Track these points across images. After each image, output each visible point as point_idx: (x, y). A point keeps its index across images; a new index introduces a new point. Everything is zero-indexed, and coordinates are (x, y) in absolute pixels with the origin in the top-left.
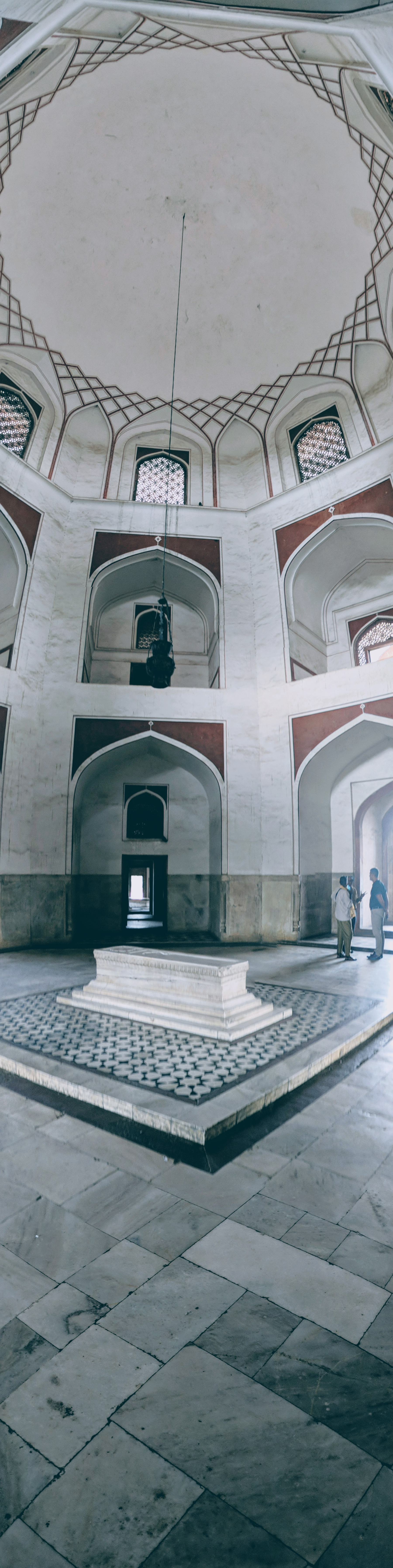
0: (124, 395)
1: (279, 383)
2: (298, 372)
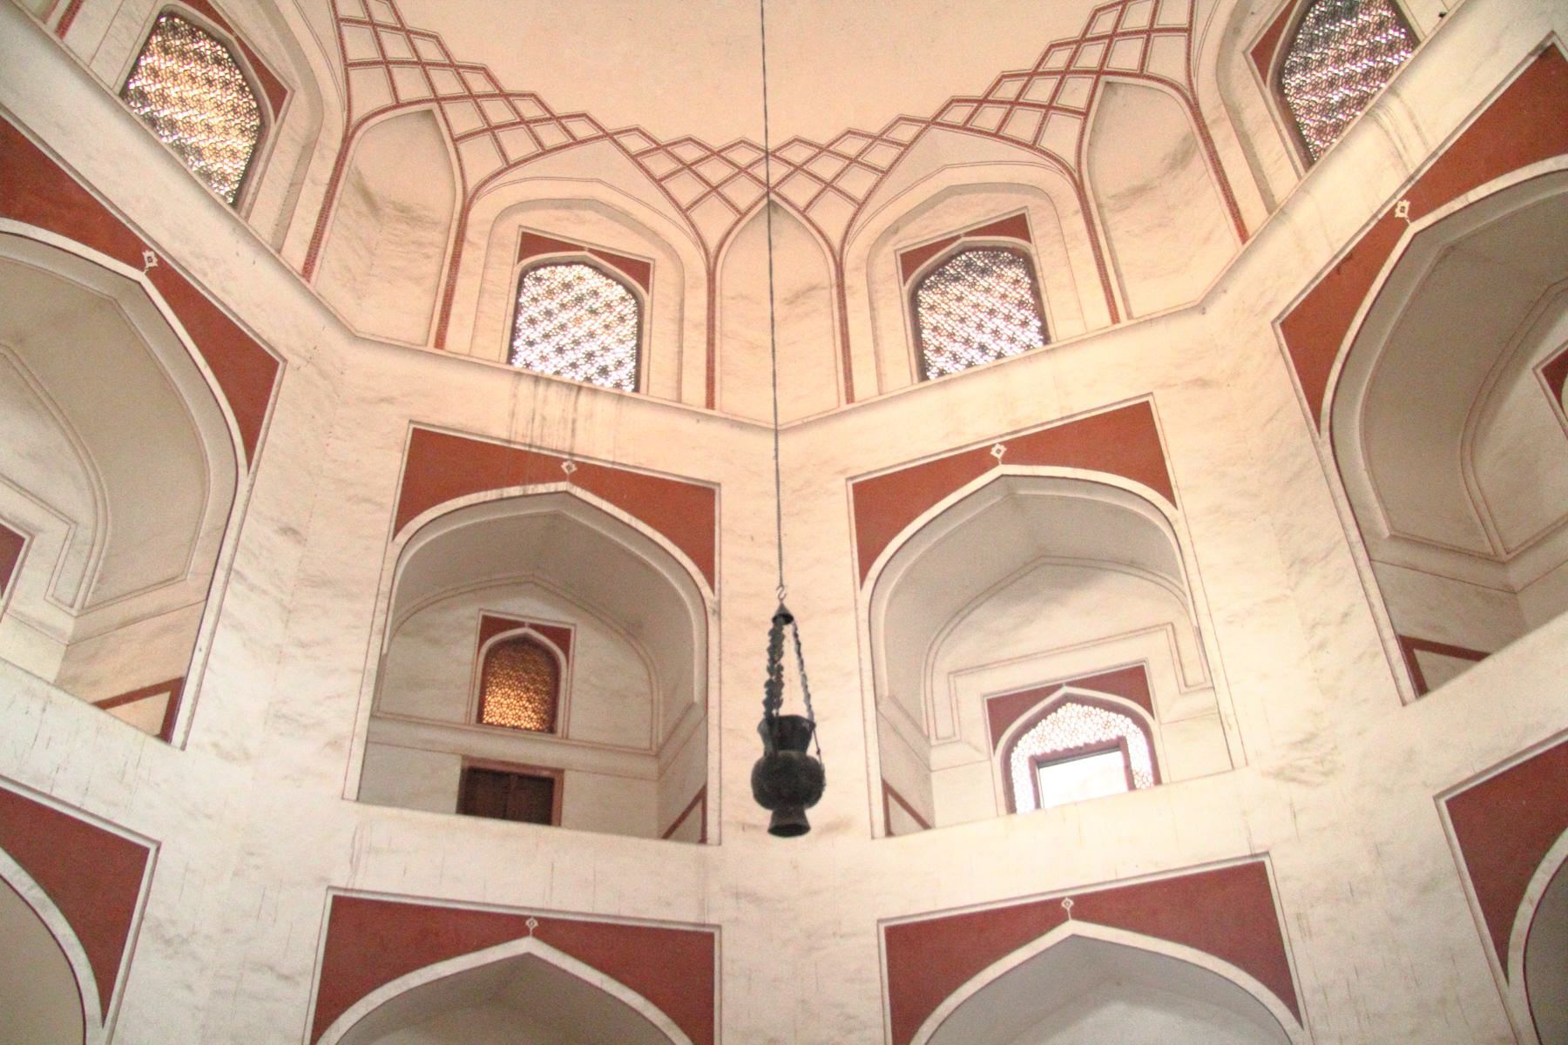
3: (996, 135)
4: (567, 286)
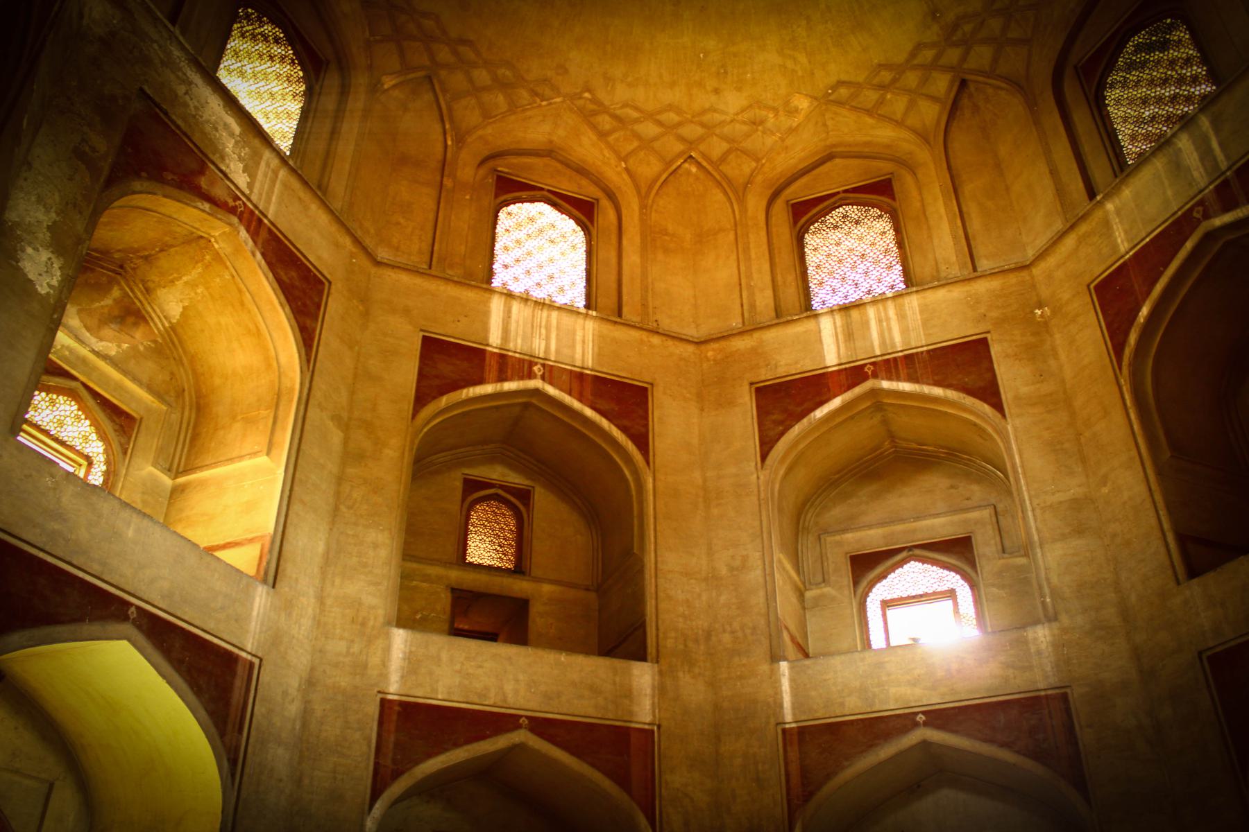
4: (532, 220)
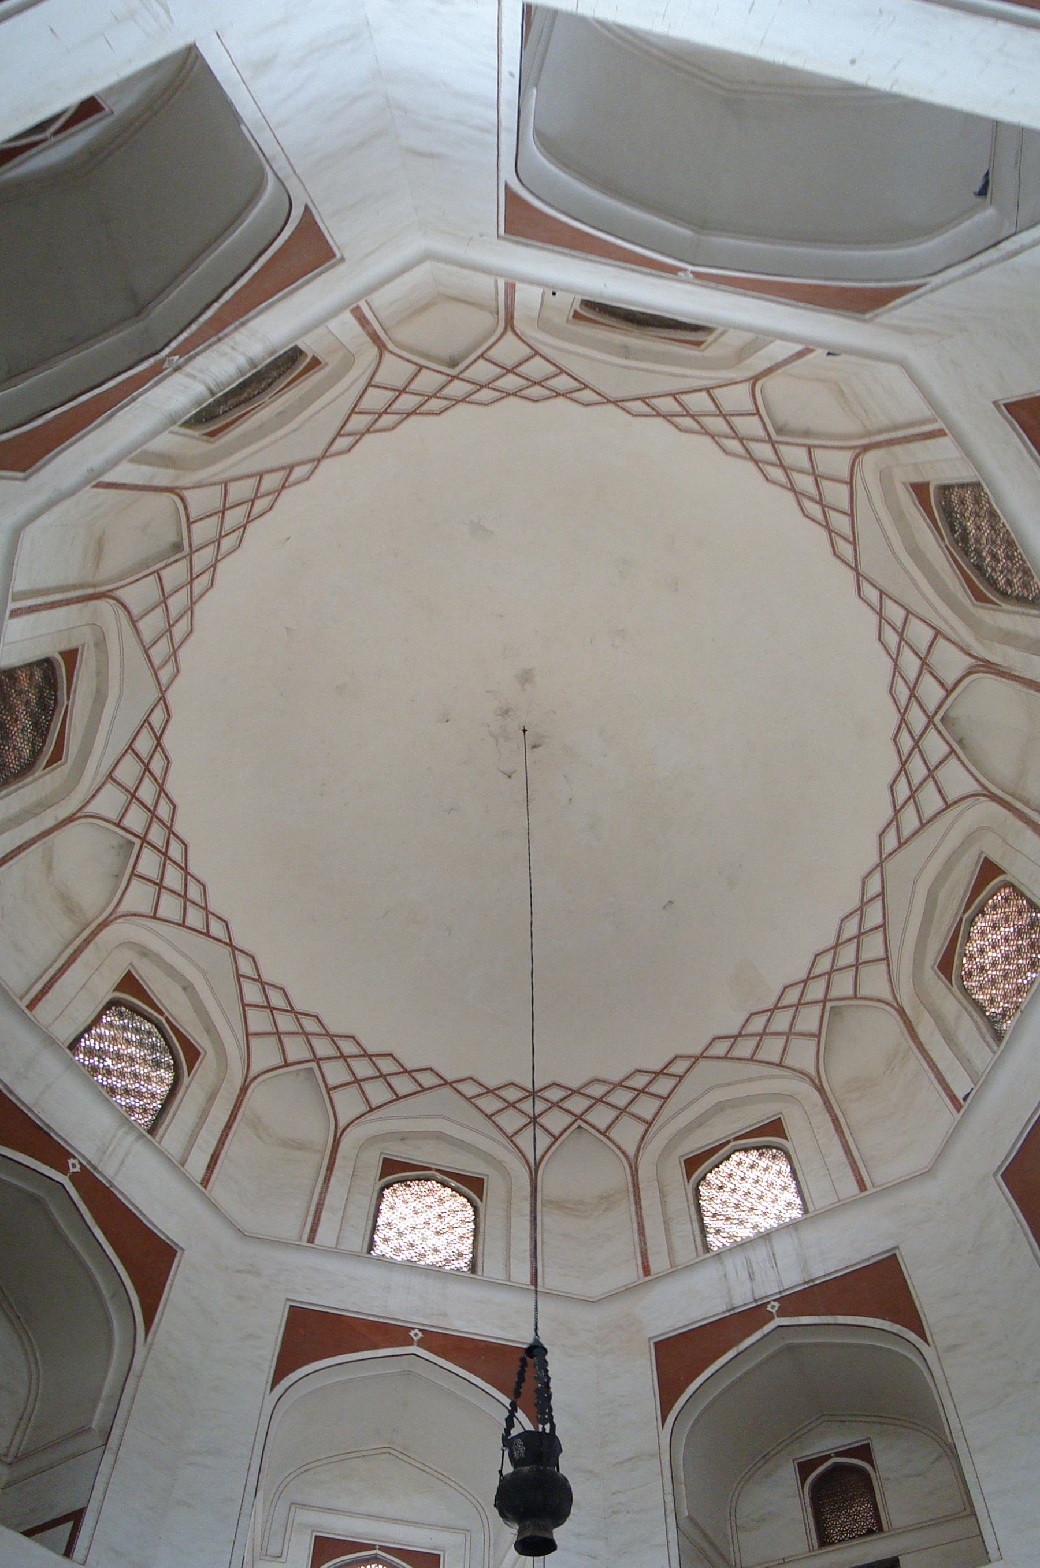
0: (185, 869)
1: (418, 1076)
2: (460, 1087)
3: (489, 1117)
